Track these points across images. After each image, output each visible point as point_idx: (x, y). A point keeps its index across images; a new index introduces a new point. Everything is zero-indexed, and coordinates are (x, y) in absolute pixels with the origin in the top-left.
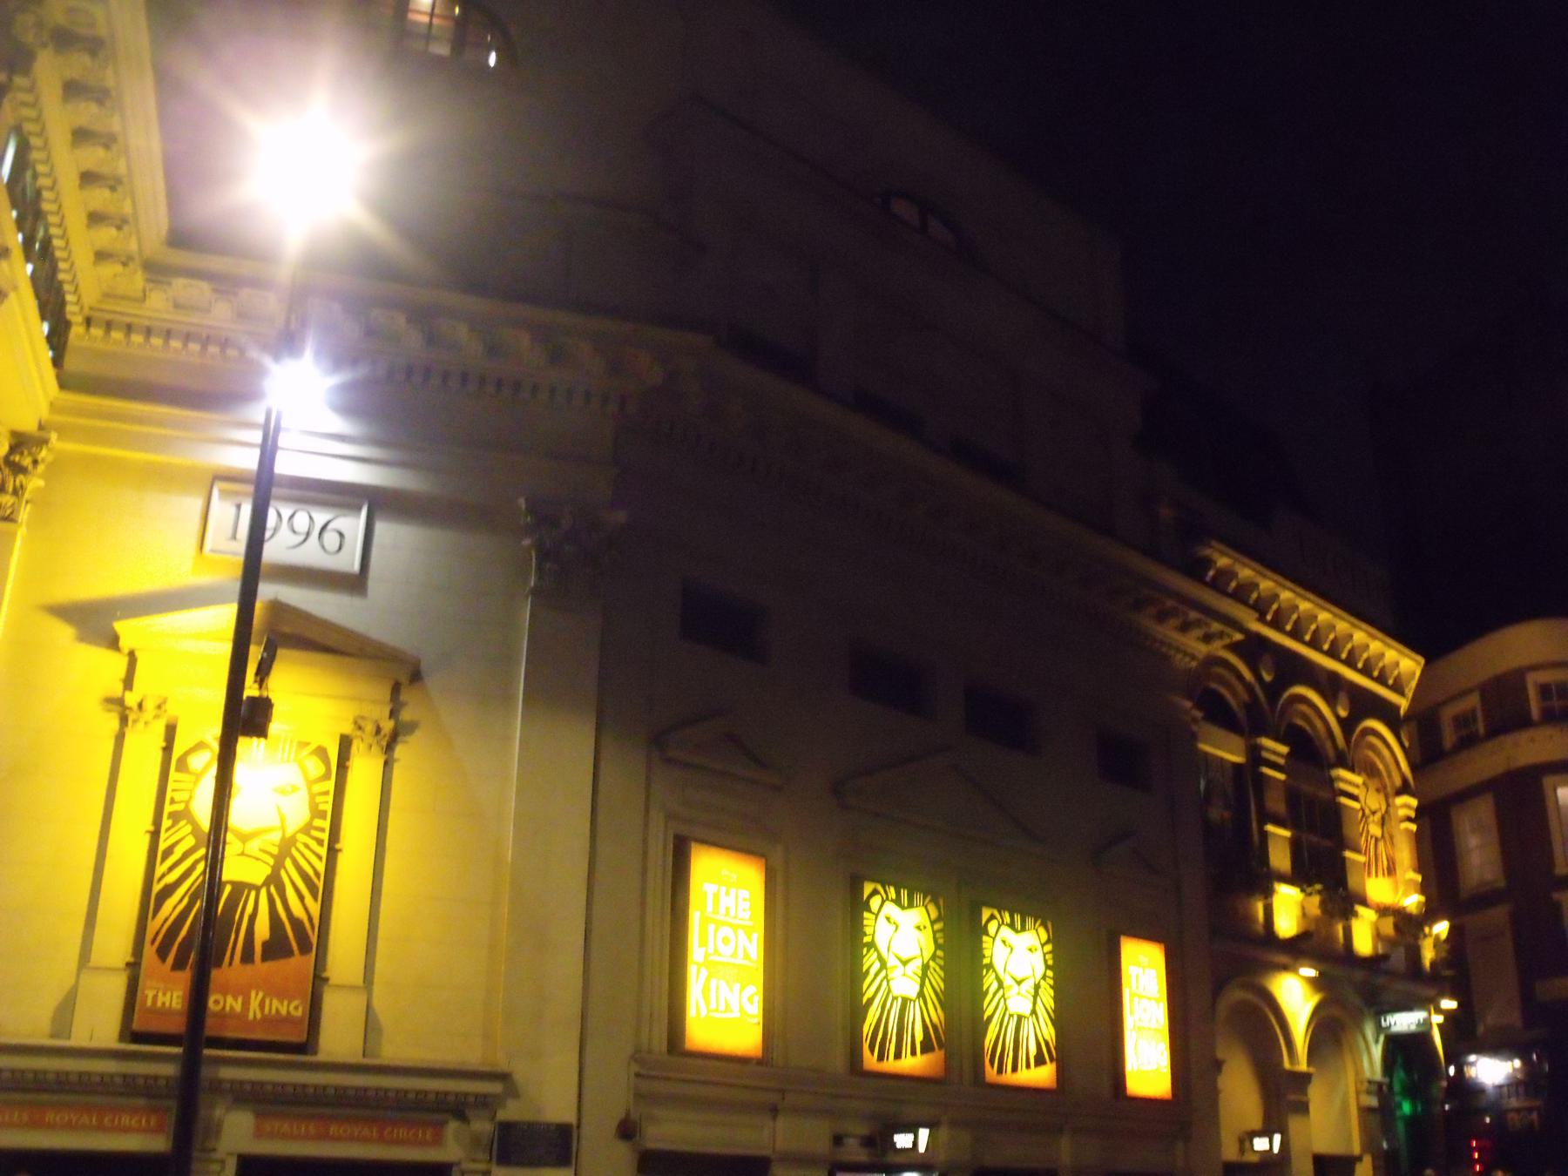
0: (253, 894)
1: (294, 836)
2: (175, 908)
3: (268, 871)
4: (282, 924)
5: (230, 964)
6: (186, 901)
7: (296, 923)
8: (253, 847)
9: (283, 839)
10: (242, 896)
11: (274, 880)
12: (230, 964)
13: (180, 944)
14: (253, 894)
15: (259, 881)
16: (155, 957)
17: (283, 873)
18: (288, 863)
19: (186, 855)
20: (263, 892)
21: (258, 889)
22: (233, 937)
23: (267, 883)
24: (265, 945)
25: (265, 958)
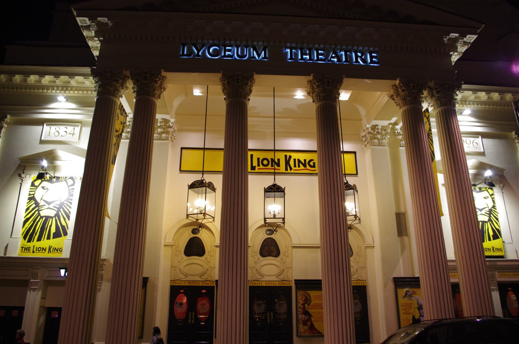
0: (51, 219)
1: (63, 202)
2: (29, 225)
3: (56, 212)
4: (59, 227)
5: (43, 240)
6: (32, 222)
7: (63, 227)
8: (51, 206)
9: (60, 203)
10: (48, 220)
11: (57, 215)
12: (43, 240)
13: (30, 234)
14: (51, 219)
15: (53, 216)
16: (23, 239)
17: (60, 213)
18: (61, 210)
19: (33, 209)
20: (54, 219)
21: (52, 218)
22: (45, 232)
23: (55, 216)
24: (54, 234)
25: (53, 238)
